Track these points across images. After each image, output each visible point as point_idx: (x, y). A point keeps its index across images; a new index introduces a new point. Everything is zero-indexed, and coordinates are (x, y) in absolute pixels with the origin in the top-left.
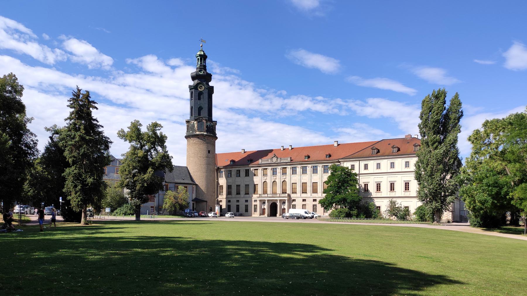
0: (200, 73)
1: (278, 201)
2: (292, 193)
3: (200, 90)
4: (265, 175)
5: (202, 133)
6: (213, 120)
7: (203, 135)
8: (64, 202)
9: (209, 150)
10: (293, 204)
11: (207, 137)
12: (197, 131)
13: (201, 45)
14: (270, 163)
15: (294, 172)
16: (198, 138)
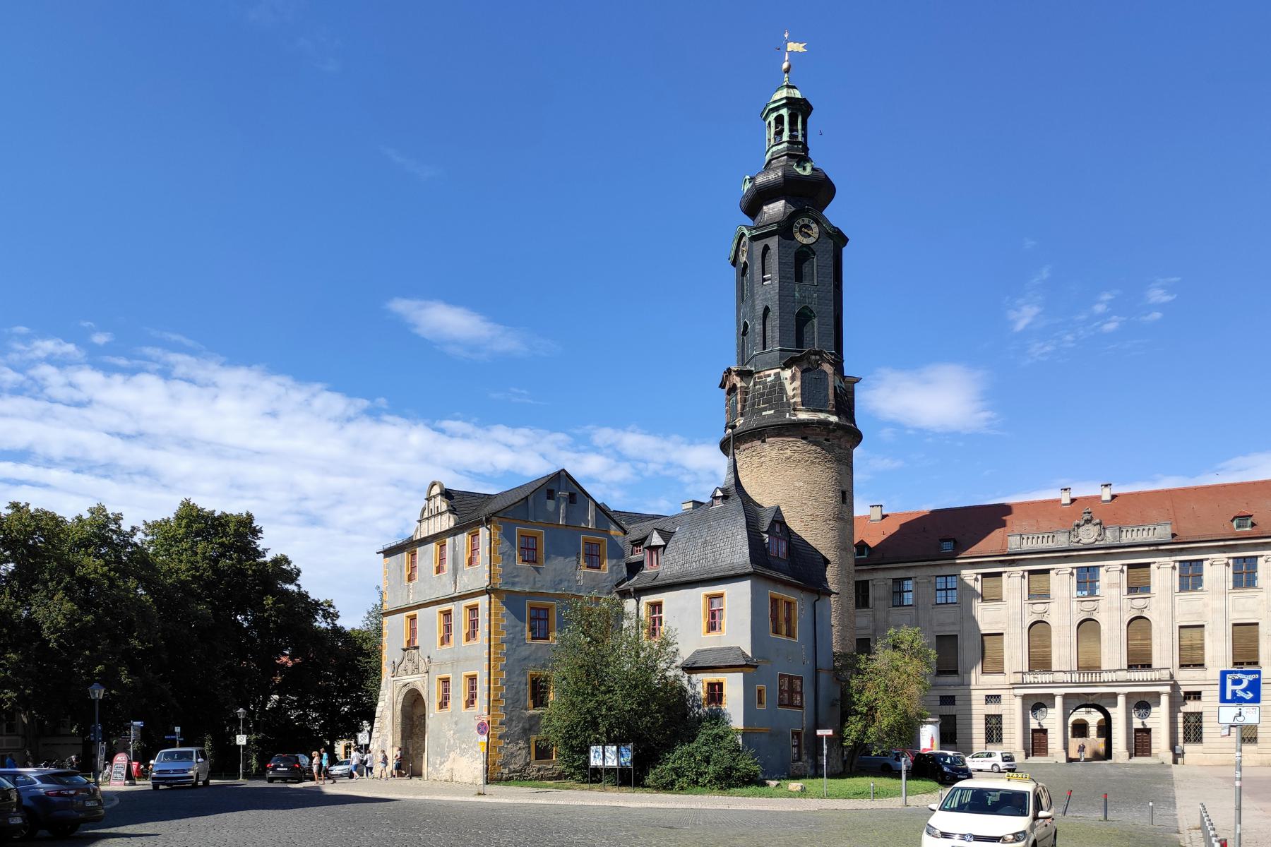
0: (799, 170)
1: (1121, 700)
2: (1182, 666)
3: (799, 238)
4: (1039, 595)
5: (822, 416)
6: (845, 375)
7: (825, 424)
8: (182, 739)
9: (845, 488)
10: (1184, 709)
11: (839, 433)
12: (800, 410)
13: (785, 65)
14: (1065, 546)
15: (1191, 578)
16: (804, 438)
